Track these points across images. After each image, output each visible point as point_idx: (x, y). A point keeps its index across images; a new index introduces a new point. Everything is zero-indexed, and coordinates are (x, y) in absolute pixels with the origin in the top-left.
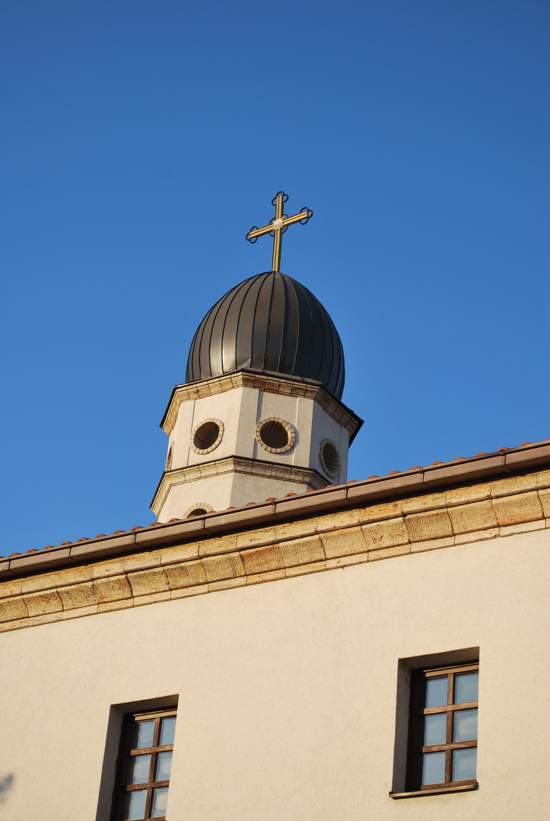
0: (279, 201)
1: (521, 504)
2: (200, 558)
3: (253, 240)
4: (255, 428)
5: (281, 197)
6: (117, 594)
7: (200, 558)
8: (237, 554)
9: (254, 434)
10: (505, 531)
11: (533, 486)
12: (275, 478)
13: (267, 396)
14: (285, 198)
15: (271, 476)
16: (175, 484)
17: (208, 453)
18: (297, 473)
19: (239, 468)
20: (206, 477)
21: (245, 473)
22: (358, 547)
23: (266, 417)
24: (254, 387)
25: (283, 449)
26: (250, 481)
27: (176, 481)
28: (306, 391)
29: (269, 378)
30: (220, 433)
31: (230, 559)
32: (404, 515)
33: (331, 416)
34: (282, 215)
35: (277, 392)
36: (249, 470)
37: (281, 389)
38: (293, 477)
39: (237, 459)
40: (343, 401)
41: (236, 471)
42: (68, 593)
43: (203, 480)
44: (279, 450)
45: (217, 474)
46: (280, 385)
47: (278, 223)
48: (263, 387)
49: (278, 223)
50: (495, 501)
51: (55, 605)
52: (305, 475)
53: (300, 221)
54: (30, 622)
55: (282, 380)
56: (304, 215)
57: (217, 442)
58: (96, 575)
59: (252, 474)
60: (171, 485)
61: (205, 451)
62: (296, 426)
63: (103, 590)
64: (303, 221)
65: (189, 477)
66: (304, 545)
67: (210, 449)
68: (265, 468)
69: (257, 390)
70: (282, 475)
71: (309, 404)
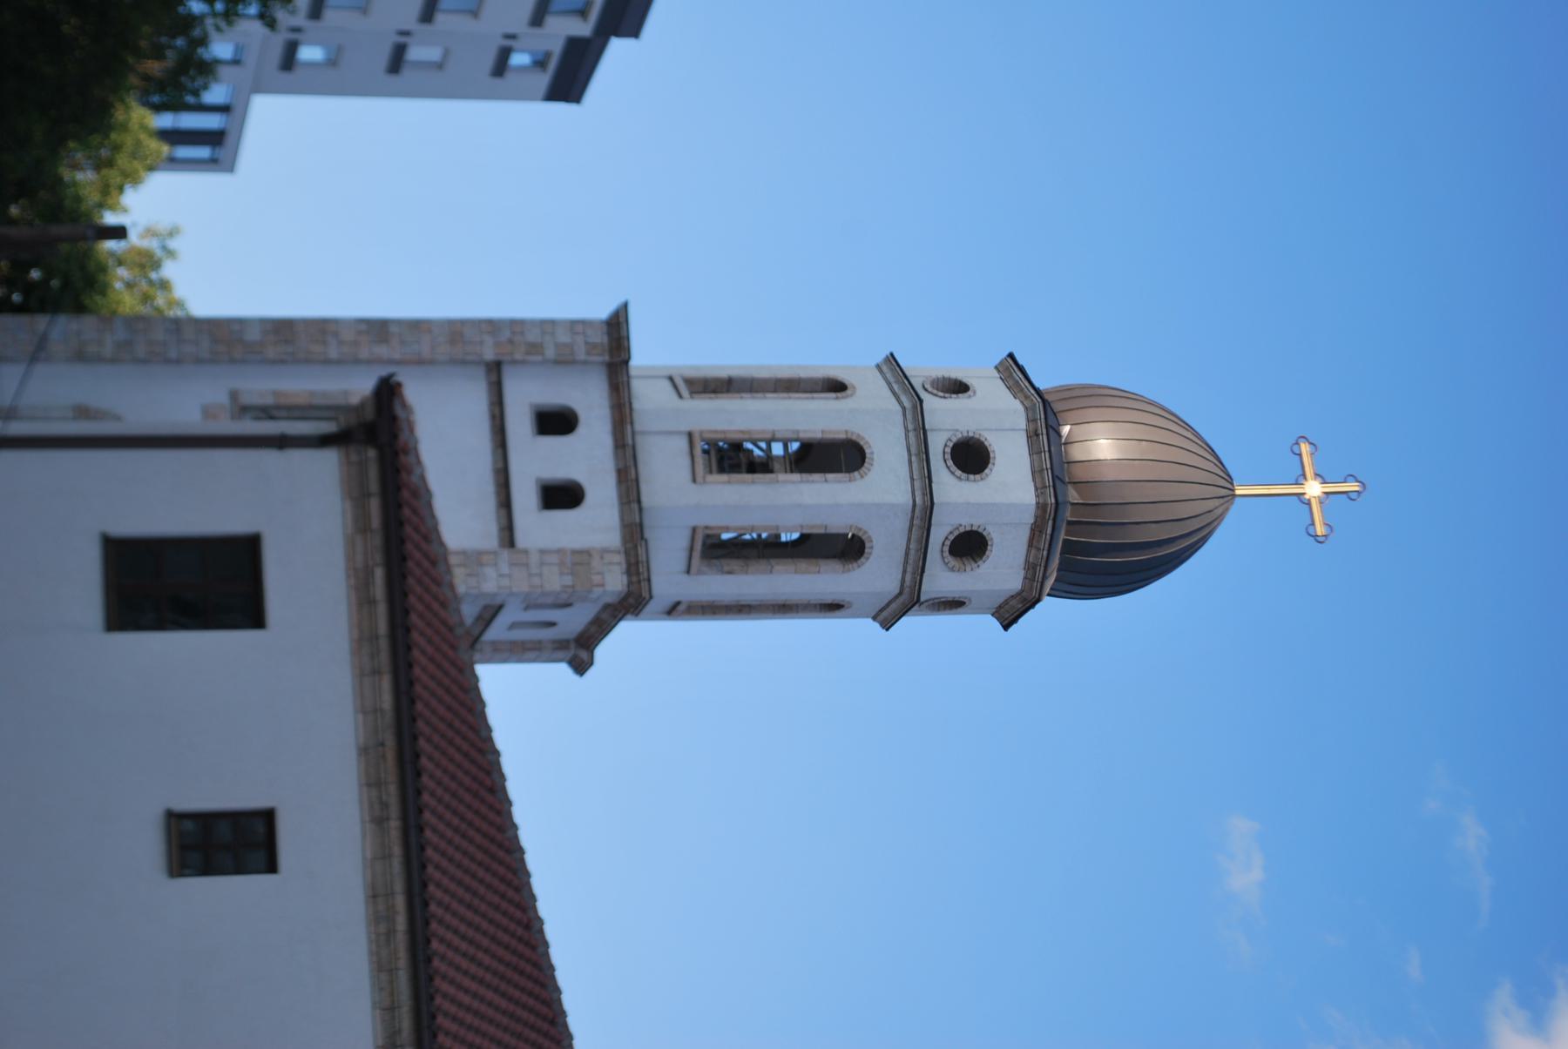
0: (1352, 487)
5: (1357, 489)
9: (967, 522)
12: (907, 554)
14: (1353, 496)
15: (909, 549)
17: (945, 461)
20: (910, 462)
21: (912, 518)
26: (901, 524)
29: (1048, 537)
33: (1006, 600)
35: (1030, 544)
37: (1033, 551)
46: (1039, 549)
47: (1313, 489)
49: (1313, 489)
53: (1313, 524)
55: (1045, 553)
56: (1320, 529)
57: (958, 473)
59: (911, 526)
61: (948, 456)
68: (919, 541)
70: (911, 561)
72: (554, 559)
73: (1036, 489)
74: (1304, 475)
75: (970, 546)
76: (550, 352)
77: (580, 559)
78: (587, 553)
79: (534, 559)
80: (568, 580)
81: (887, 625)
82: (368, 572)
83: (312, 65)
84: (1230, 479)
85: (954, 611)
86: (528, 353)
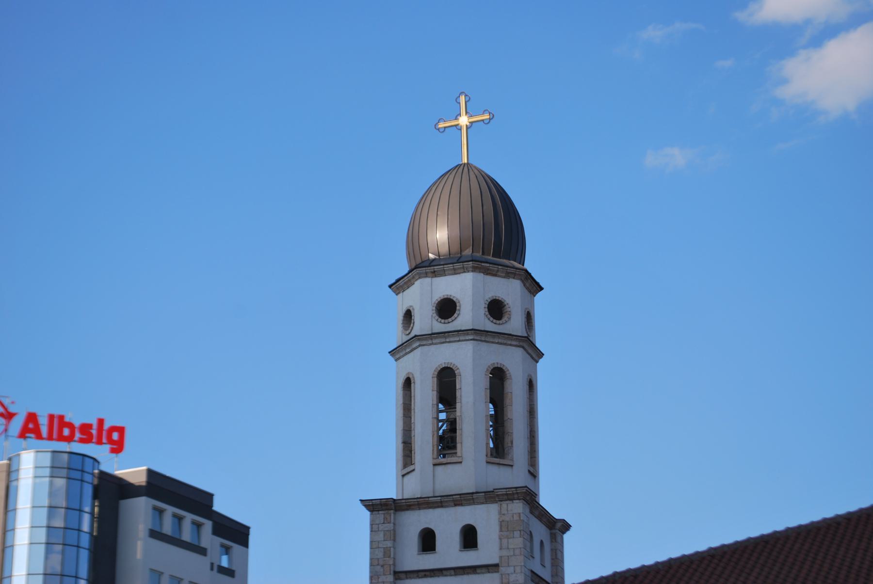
0: (462, 99)
3: (442, 130)
5: (463, 97)
9: (483, 310)
12: (501, 344)
14: (467, 99)
15: (498, 342)
17: (449, 323)
20: (450, 342)
26: (484, 347)
29: (491, 265)
33: (526, 289)
34: (466, 113)
35: (495, 275)
37: (499, 274)
43: (447, 344)
46: (498, 271)
47: (464, 120)
49: (464, 120)
53: (483, 120)
55: (500, 267)
56: (486, 117)
57: (455, 315)
61: (446, 321)
64: (486, 122)
68: (494, 337)
70: (505, 342)
72: (505, 541)
73: (464, 272)
74: (456, 126)
75: (496, 309)
76: (389, 544)
77: (505, 527)
78: (501, 523)
79: (505, 553)
80: (517, 534)
81: (541, 355)
83: (230, 561)
85: (532, 318)
86: (389, 557)
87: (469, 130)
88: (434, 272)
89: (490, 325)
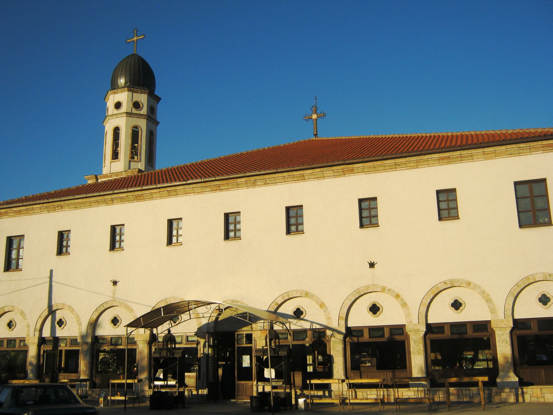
0: (135, 31)
1: (190, 190)
2: (127, 196)
4: (131, 104)
6: (110, 202)
7: (127, 196)
8: (135, 196)
9: (131, 105)
10: (187, 195)
11: (192, 187)
13: (134, 94)
16: (110, 119)
18: (143, 116)
19: (127, 115)
22: (159, 196)
23: (134, 100)
24: (131, 92)
25: (139, 109)
26: (131, 119)
27: (109, 118)
28: (145, 92)
30: (122, 105)
31: (134, 197)
32: (168, 191)
34: (136, 36)
35: (137, 93)
36: (130, 116)
37: (138, 92)
38: (142, 117)
39: (127, 113)
40: (155, 93)
41: (127, 116)
42: (100, 201)
43: (118, 118)
44: (138, 110)
45: (122, 117)
47: (135, 38)
48: (133, 92)
50: (185, 189)
51: (97, 204)
52: (145, 116)
53: (142, 38)
54: (92, 206)
56: (143, 37)
57: (121, 108)
58: (105, 198)
59: (131, 117)
60: (109, 119)
62: (143, 102)
63: (107, 201)
65: (114, 117)
66: (148, 195)
67: (119, 109)
69: (132, 93)
71: (146, 96)
73: (125, 92)
75: (137, 105)
81: (158, 123)
82: (15, 212)
84: (134, 54)
87: (138, 42)
88: (115, 92)
89: (134, 111)
